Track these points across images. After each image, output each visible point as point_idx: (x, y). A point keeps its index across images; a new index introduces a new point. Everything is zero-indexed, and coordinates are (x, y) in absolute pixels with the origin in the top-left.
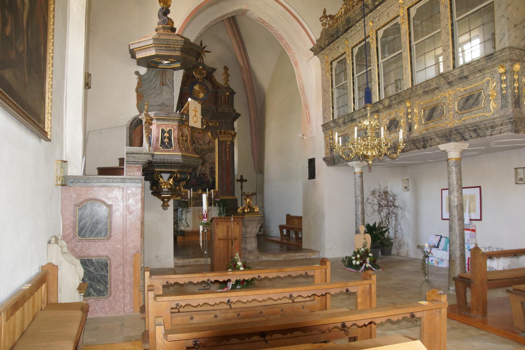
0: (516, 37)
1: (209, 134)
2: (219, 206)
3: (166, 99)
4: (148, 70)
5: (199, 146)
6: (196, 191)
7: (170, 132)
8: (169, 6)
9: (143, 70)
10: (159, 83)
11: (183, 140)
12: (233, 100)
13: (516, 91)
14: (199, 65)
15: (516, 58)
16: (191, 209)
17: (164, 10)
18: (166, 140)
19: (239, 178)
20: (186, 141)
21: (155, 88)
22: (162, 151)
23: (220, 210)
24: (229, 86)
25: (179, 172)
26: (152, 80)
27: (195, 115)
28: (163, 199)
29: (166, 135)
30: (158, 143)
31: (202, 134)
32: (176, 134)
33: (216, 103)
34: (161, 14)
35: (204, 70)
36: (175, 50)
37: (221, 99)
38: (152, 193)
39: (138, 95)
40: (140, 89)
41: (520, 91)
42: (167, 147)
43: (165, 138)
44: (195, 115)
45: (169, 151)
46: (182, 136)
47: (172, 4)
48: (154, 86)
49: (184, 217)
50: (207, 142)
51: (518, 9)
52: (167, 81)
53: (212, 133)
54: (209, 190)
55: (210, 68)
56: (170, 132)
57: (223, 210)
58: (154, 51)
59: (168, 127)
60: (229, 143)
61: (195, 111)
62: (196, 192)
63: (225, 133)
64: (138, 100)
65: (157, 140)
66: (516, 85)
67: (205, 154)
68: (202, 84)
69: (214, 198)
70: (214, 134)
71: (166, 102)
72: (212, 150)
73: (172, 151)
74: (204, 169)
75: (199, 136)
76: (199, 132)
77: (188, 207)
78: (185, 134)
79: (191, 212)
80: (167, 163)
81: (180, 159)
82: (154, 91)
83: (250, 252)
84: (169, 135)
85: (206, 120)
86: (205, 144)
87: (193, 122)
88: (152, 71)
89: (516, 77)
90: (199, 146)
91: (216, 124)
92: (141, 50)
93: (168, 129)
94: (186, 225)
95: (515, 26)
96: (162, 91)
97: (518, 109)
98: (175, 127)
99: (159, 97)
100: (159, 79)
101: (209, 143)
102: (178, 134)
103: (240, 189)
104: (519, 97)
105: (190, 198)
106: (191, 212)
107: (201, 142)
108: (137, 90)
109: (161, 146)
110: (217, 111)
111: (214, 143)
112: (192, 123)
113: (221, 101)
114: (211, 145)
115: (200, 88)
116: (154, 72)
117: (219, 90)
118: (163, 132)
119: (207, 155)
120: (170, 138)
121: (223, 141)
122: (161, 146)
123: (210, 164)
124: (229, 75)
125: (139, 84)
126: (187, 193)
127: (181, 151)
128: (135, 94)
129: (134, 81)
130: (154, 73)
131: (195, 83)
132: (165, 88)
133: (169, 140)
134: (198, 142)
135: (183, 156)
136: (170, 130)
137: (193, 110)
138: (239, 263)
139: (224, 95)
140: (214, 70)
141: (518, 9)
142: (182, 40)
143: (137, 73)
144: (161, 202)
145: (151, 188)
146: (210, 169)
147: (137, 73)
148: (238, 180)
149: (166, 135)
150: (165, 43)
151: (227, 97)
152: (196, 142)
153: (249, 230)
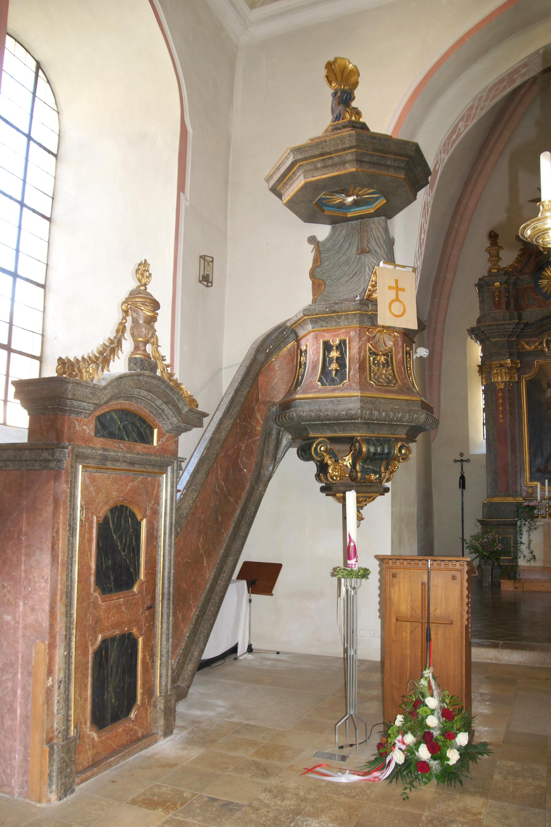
4: (333, 229)
7: (341, 347)
8: (356, 84)
9: (322, 231)
10: (355, 250)
16: (540, 522)
17: (339, 94)
18: (334, 366)
22: (319, 391)
25: (368, 441)
27: (397, 299)
30: (316, 375)
36: (345, 163)
39: (314, 284)
40: (318, 270)
42: (333, 382)
44: (397, 299)
45: (334, 390)
48: (344, 258)
49: (525, 539)
52: (373, 243)
56: (341, 347)
58: (302, 177)
59: (337, 336)
64: (314, 295)
65: (314, 367)
73: (342, 390)
77: (533, 517)
79: (540, 530)
80: (327, 418)
82: (346, 268)
84: (341, 353)
87: (388, 315)
88: (342, 230)
92: (286, 184)
93: (337, 342)
94: (529, 556)
98: (352, 334)
99: (355, 279)
105: (543, 498)
106: (540, 530)
108: (312, 275)
109: (320, 380)
112: (385, 318)
116: (343, 228)
118: (327, 347)
122: (320, 380)
125: (315, 260)
126: (534, 488)
128: (309, 283)
129: (308, 255)
130: (344, 232)
133: (340, 366)
135: (363, 399)
137: (403, 290)
138: (432, 702)
142: (350, 136)
143: (312, 240)
147: (312, 240)
149: (334, 354)
150: (318, 152)
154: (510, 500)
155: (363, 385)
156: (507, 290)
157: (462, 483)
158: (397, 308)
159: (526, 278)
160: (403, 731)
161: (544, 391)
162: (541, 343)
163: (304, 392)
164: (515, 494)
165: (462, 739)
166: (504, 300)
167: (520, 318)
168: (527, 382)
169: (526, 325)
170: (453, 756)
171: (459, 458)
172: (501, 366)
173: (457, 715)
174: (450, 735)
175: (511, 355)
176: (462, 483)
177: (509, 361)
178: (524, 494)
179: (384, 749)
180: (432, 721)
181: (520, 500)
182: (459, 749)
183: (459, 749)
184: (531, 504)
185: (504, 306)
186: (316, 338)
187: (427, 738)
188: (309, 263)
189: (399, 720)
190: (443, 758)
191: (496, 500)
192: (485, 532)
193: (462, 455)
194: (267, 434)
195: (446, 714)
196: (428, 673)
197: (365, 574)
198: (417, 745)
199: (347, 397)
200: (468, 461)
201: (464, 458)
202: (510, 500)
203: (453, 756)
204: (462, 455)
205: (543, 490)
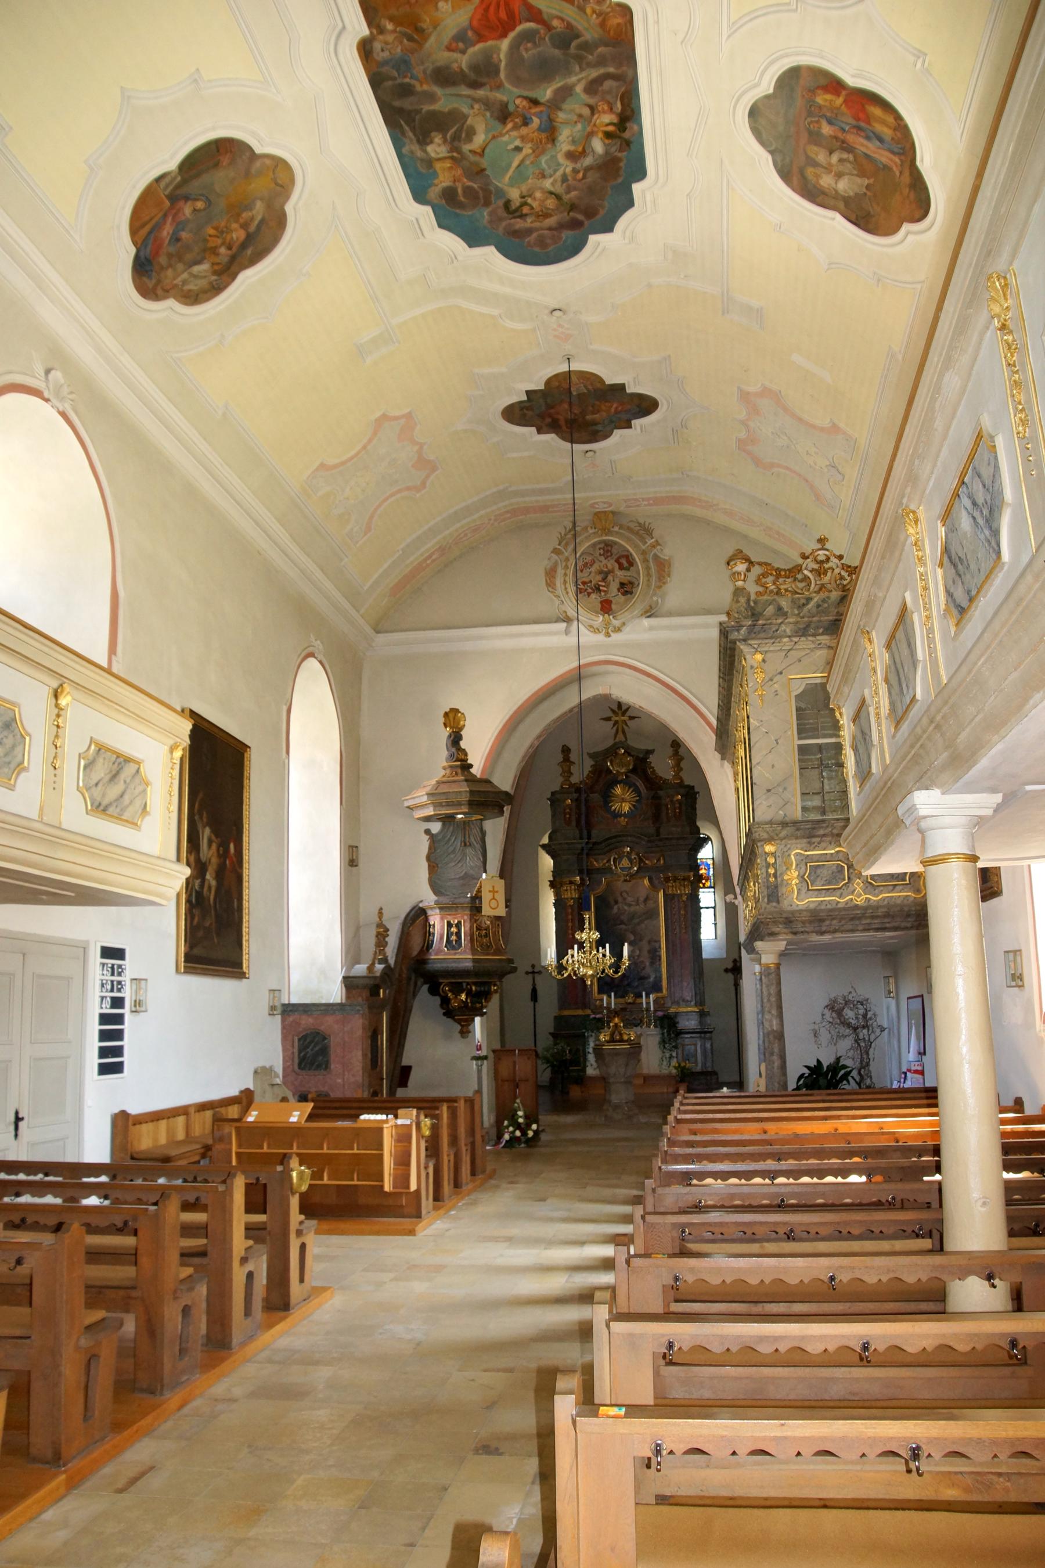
0: (770, 806)
1: (646, 882)
2: (662, 1027)
3: (472, 868)
4: (444, 825)
5: (626, 908)
6: (623, 997)
11: (480, 936)
12: (695, 809)
13: (772, 879)
14: (618, 748)
15: (765, 836)
18: (454, 938)
19: (730, 966)
20: (486, 936)
21: (453, 852)
22: (446, 954)
23: (663, 1034)
24: (682, 781)
25: (475, 984)
26: (449, 839)
27: (494, 898)
28: (459, 1022)
29: (454, 930)
31: (630, 884)
32: (468, 928)
33: (656, 818)
34: (450, 742)
35: (630, 755)
37: (667, 809)
38: (444, 1014)
39: (429, 866)
41: (779, 879)
42: (454, 948)
43: (452, 934)
44: (494, 898)
45: (455, 954)
46: (478, 929)
47: (467, 723)
48: (451, 849)
50: (642, 899)
51: (773, 766)
53: (650, 880)
54: (647, 996)
55: (639, 751)
57: (669, 1034)
58: (432, 809)
60: (685, 898)
61: (494, 892)
62: (621, 1000)
63: (675, 879)
65: (442, 938)
66: (772, 871)
67: (639, 924)
68: (627, 784)
69: (655, 1011)
70: (656, 882)
71: (471, 872)
72: (653, 914)
73: (460, 954)
74: (638, 952)
75: (627, 887)
76: (625, 881)
78: (483, 925)
81: (469, 965)
83: (616, 1107)
85: (638, 855)
86: (638, 904)
89: (771, 860)
90: (626, 908)
91: (659, 860)
95: (769, 791)
96: (465, 855)
97: (774, 904)
100: (460, 838)
101: (646, 899)
102: (471, 928)
103: (733, 988)
104: (776, 887)
107: (629, 899)
108: (428, 858)
110: (658, 834)
111: (657, 902)
112: (486, 910)
113: (667, 813)
114: (650, 904)
115: (623, 789)
117: (661, 793)
118: (450, 925)
119: (643, 926)
120: (458, 934)
121: (674, 896)
123: (649, 942)
124: (682, 759)
125: (430, 848)
126: (602, 1000)
127: (473, 954)
128: (426, 865)
130: (451, 828)
131: (615, 782)
132: (469, 850)
134: (625, 899)
135: (474, 961)
136: (459, 923)
138: (520, 1113)
139: (672, 801)
140: (651, 752)
141: (773, 766)
143: (427, 832)
144: (459, 1027)
145: (442, 1006)
146: (649, 952)
147: (427, 832)
148: (726, 970)
149: (454, 930)
151: (677, 805)
152: (620, 899)
153: (612, 1070)
154: (580, 1012)
155: (474, 951)
156: (578, 807)
157: (534, 996)
158: (493, 904)
159: (596, 797)
160: (507, 1127)
161: (612, 908)
162: (609, 861)
163: (436, 954)
164: (584, 1006)
165: (534, 1127)
166: (574, 818)
167: (589, 837)
168: (596, 899)
169: (595, 844)
170: (531, 1134)
171: (530, 970)
172: (571, 883)
173: (530, 1118)
174: (528, 1126)
175: (581, 872)
176: (534, 996)
177: (578, 878)
178: (592, 1007)
179: (500, 1137)
180: (521, 1120)
181: (589, 1012)
182: (535, 1132)
183: (535, 1132)
184: (598, 1016)
185: (574, 823)
186: (442, 919)
187: (518, 1126)
188: (425, 850)
189: (506, 1123)
190: (527, 1134)
191: (566, 1013)
192: (556, 1044)
193: (533, 966)
194: (409, 979)
195: (526, 1117)
196: (518, 1101)
197: (486, 1058)
198: (514, 1132)
199: (464, 957)
200: (540, 973)
201: (536, 970)
202: (580, 1012)
203: (531, 1134)
204: (533, 966)
205: (609, 1003)
